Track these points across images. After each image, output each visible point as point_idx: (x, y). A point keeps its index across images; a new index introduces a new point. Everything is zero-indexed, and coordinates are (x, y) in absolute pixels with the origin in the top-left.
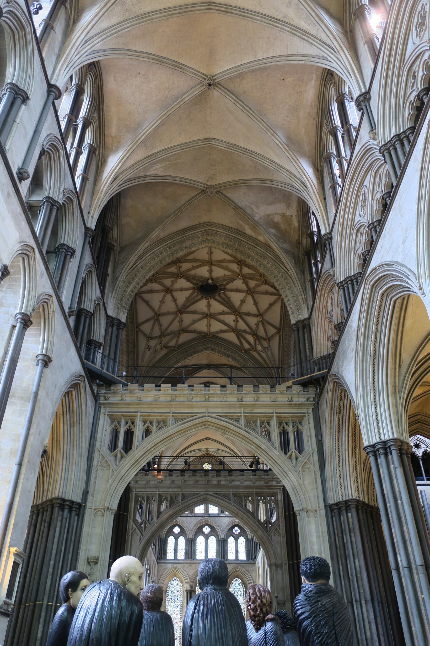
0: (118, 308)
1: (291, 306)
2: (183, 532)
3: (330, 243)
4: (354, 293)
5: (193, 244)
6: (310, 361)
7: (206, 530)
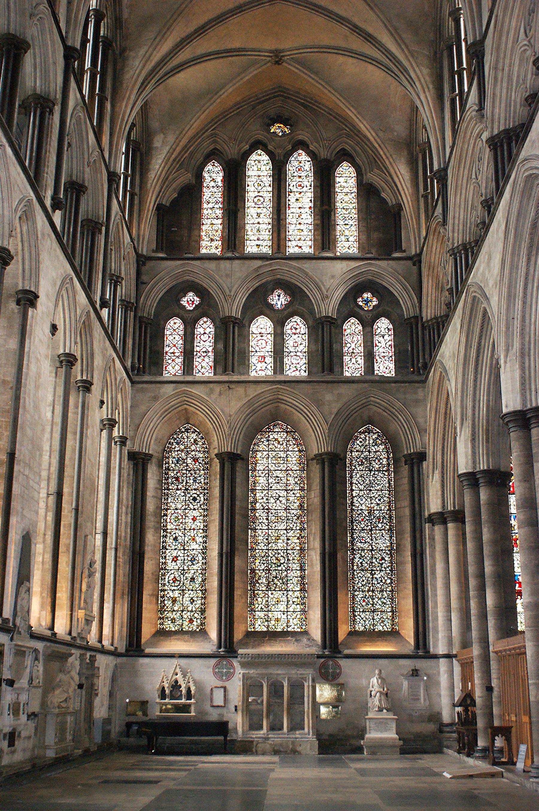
2: (209, 306)
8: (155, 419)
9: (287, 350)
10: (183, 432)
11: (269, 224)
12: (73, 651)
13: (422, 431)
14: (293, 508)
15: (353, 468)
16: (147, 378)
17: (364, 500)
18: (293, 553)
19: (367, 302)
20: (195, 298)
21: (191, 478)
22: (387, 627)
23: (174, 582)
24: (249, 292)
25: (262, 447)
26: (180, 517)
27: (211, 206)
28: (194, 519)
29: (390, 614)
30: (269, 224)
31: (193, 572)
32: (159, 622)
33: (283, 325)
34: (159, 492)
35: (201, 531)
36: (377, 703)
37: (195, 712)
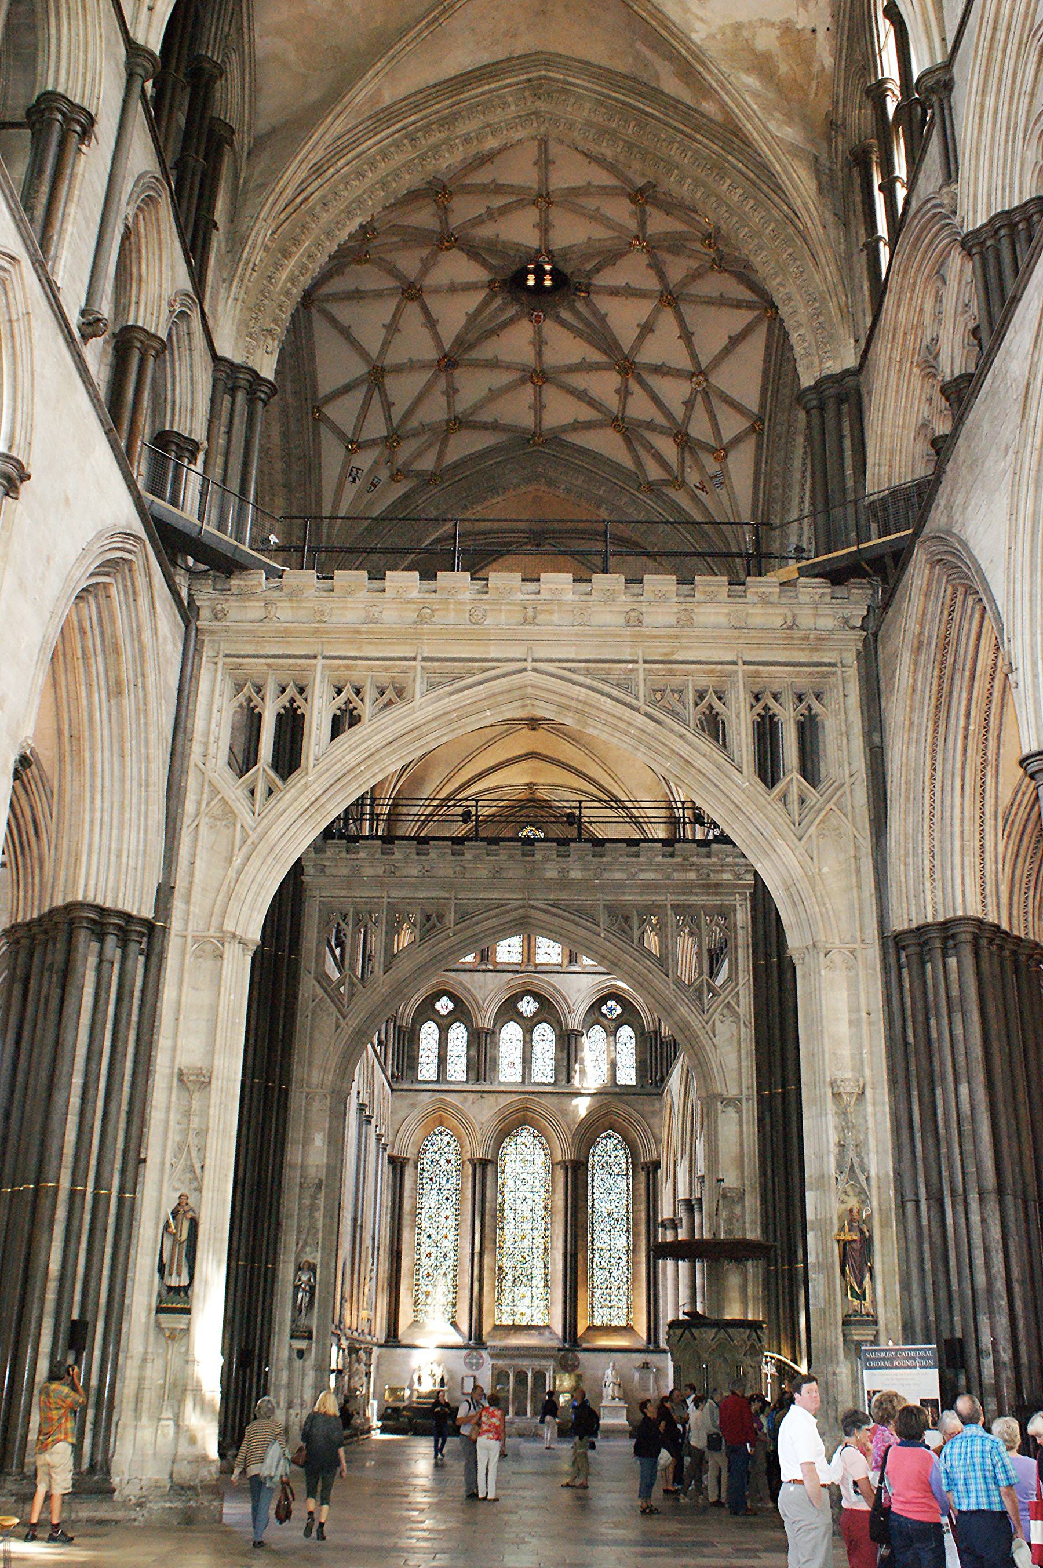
0: (250, 335)
1: (802, 331)
3: (945, 101)
4: (1016, 270)
5: (489, 126)
6: (855, 502)
7: (528, 1006)
19: (611, 1010)
22: (623, 1323)
25: (510, 1150)
36: (610, 1392)
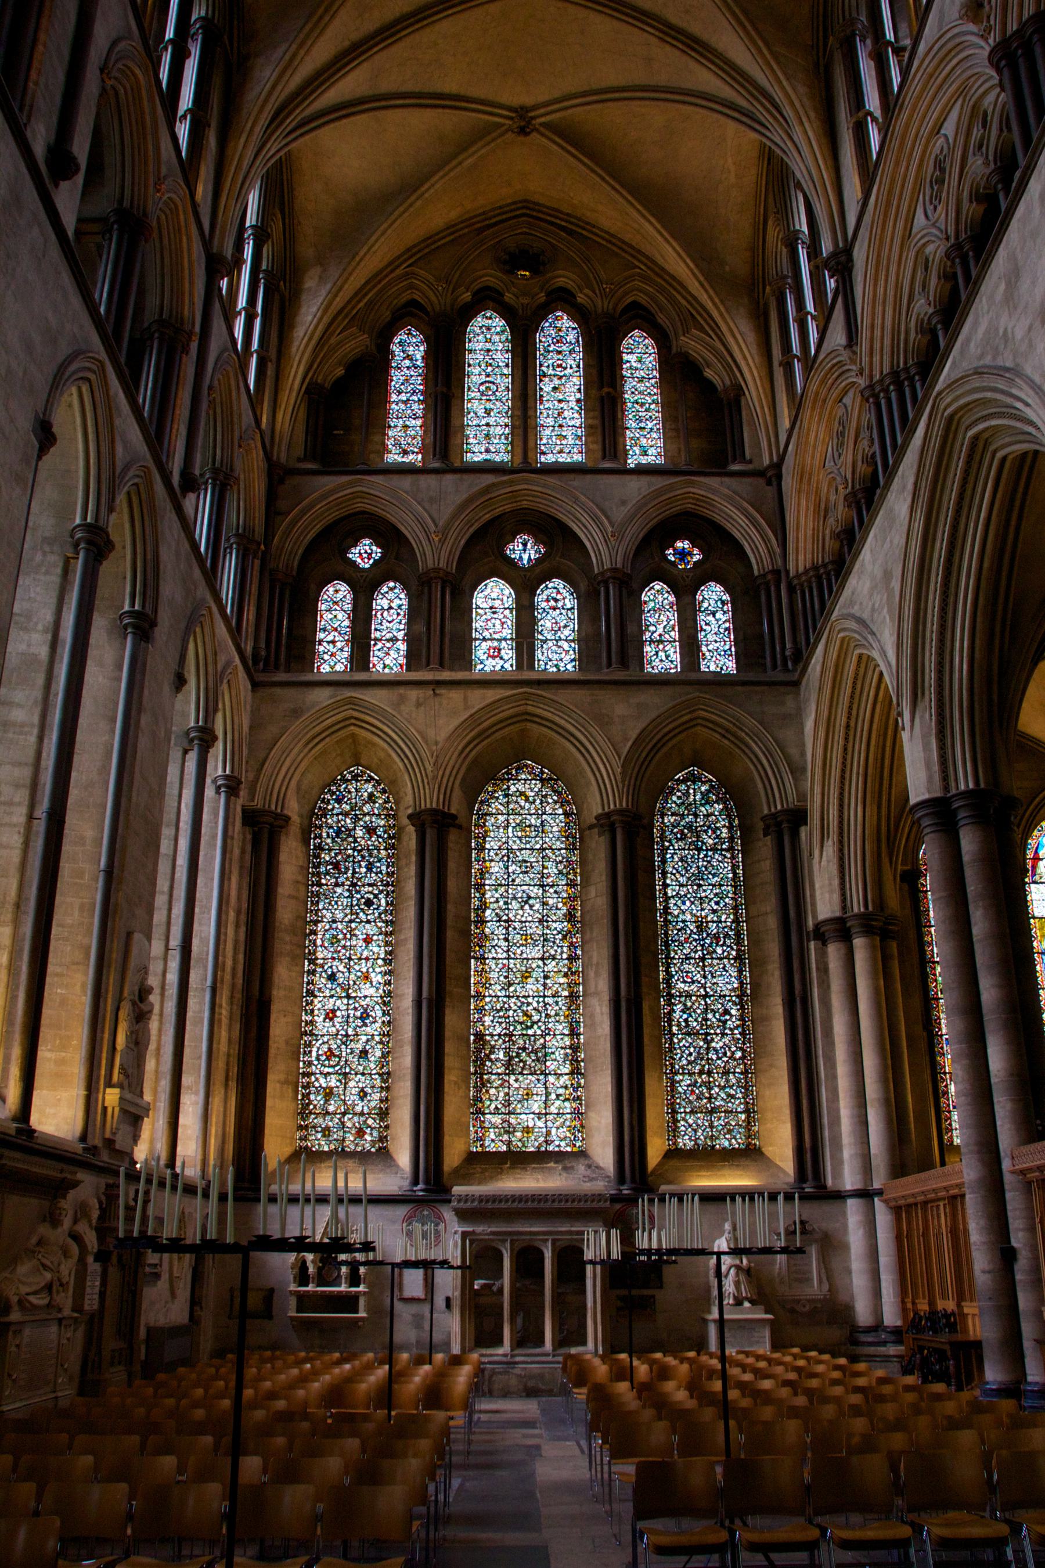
8: (296, 751)
9: (540, 637)
10: (348, 780)
11: (506, 426)
12: (81, 1175)
13: (797, 771)
14: (554, 918)
15: (667, 844)
16: (282, 676)
17: (688, 903)
18: (557, 1003)
19: (683, 554)
20: (374, 548)
21: (363, 864)
22: (738, 1142)
23: (328, 1059)
24: (471, 530)
25: (495, 806)
26: (341, 936)
27: (403, 397)
28: (368, 940)
29: (743, 1116)
30: (506, 426)
31: (364, 1038)
32: (298, 1135)
33: (533, 594)
34: (302, 888)
35: (380, 962)
37: (367, 1311)
